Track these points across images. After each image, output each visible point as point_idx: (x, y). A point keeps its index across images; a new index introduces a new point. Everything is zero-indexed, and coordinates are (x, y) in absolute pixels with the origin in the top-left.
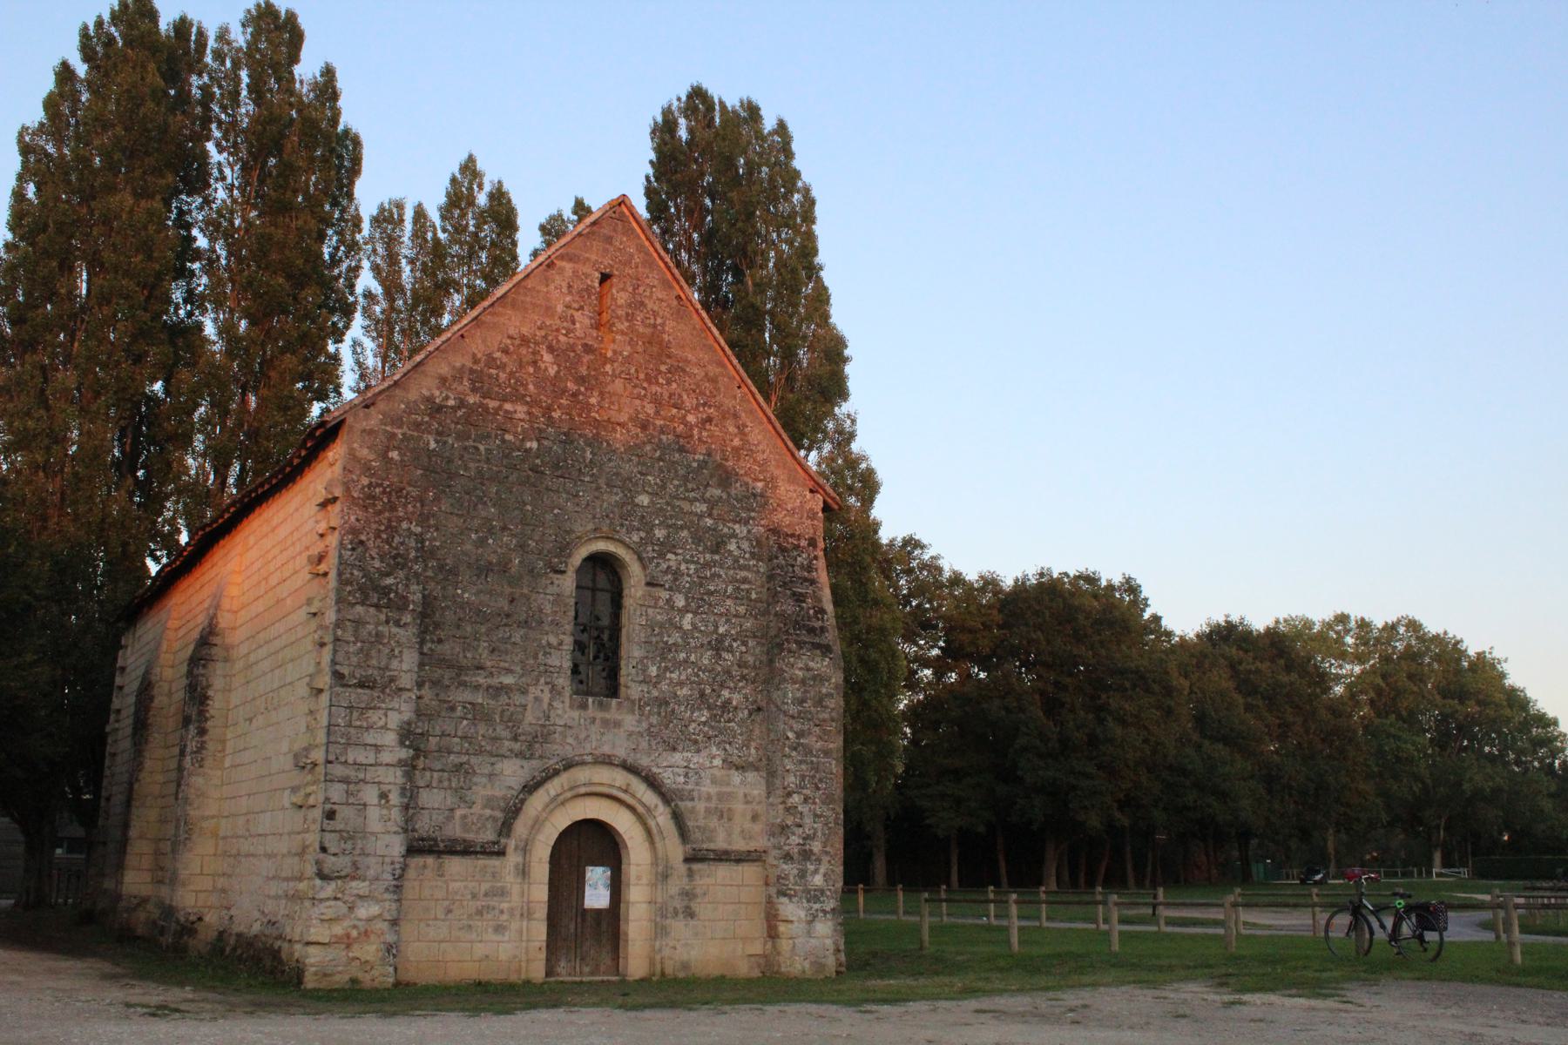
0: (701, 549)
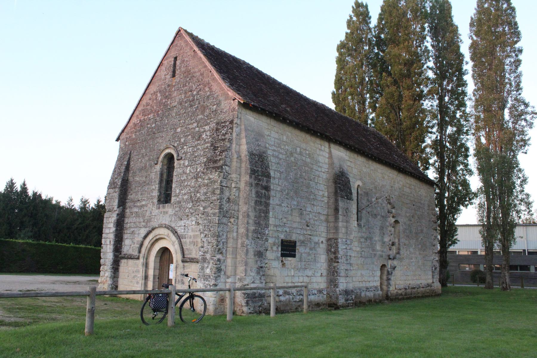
0: (194, 141)
